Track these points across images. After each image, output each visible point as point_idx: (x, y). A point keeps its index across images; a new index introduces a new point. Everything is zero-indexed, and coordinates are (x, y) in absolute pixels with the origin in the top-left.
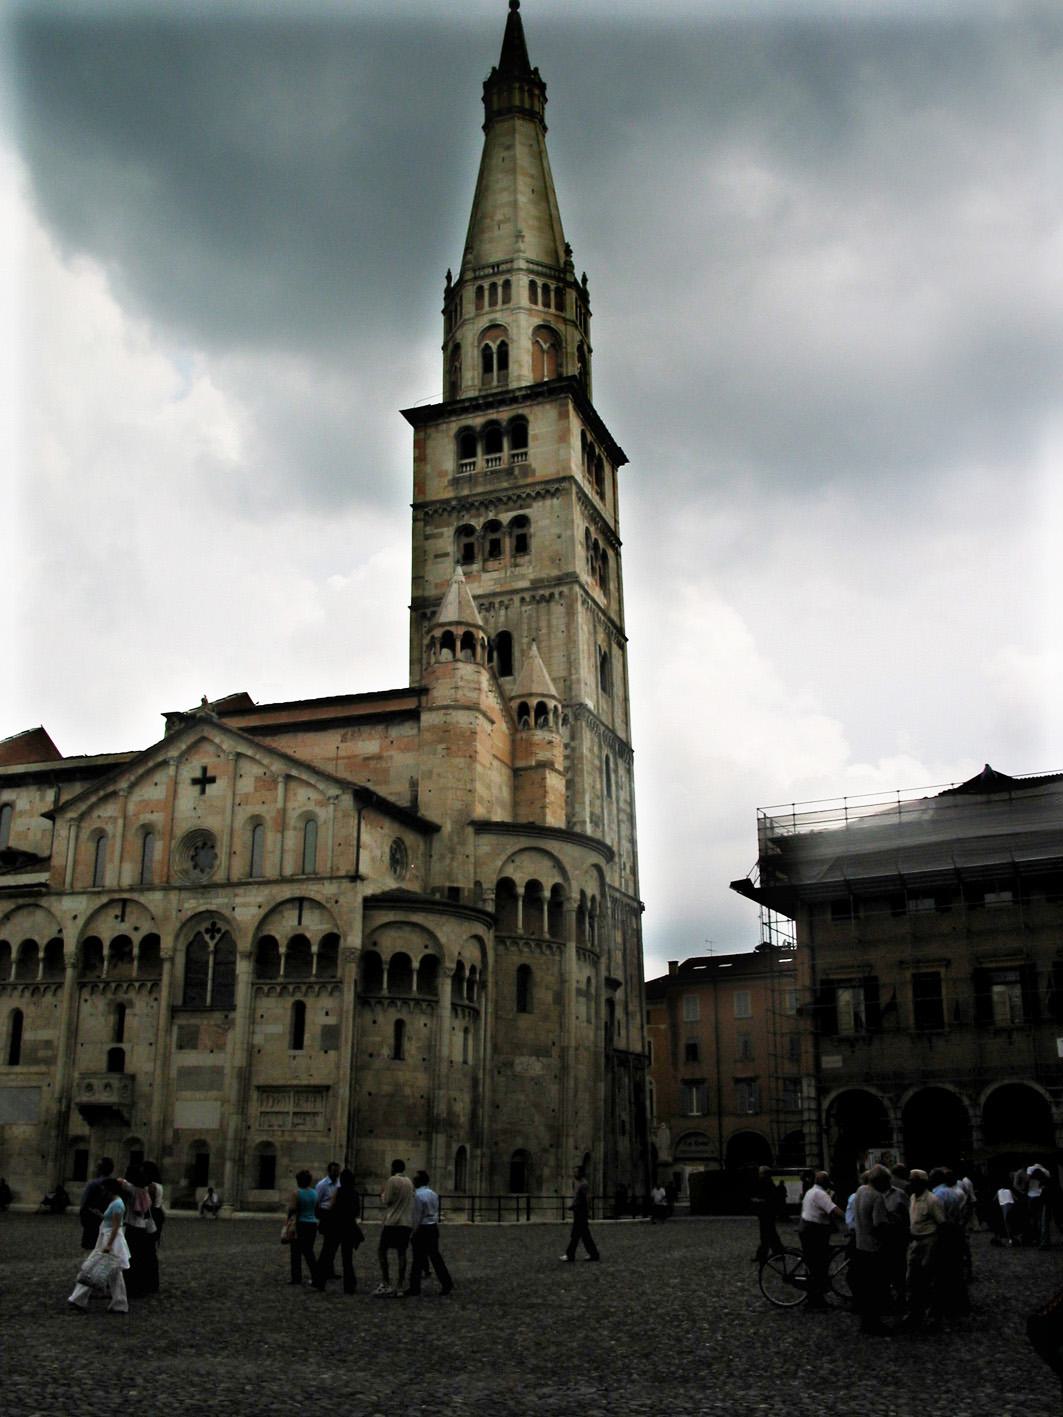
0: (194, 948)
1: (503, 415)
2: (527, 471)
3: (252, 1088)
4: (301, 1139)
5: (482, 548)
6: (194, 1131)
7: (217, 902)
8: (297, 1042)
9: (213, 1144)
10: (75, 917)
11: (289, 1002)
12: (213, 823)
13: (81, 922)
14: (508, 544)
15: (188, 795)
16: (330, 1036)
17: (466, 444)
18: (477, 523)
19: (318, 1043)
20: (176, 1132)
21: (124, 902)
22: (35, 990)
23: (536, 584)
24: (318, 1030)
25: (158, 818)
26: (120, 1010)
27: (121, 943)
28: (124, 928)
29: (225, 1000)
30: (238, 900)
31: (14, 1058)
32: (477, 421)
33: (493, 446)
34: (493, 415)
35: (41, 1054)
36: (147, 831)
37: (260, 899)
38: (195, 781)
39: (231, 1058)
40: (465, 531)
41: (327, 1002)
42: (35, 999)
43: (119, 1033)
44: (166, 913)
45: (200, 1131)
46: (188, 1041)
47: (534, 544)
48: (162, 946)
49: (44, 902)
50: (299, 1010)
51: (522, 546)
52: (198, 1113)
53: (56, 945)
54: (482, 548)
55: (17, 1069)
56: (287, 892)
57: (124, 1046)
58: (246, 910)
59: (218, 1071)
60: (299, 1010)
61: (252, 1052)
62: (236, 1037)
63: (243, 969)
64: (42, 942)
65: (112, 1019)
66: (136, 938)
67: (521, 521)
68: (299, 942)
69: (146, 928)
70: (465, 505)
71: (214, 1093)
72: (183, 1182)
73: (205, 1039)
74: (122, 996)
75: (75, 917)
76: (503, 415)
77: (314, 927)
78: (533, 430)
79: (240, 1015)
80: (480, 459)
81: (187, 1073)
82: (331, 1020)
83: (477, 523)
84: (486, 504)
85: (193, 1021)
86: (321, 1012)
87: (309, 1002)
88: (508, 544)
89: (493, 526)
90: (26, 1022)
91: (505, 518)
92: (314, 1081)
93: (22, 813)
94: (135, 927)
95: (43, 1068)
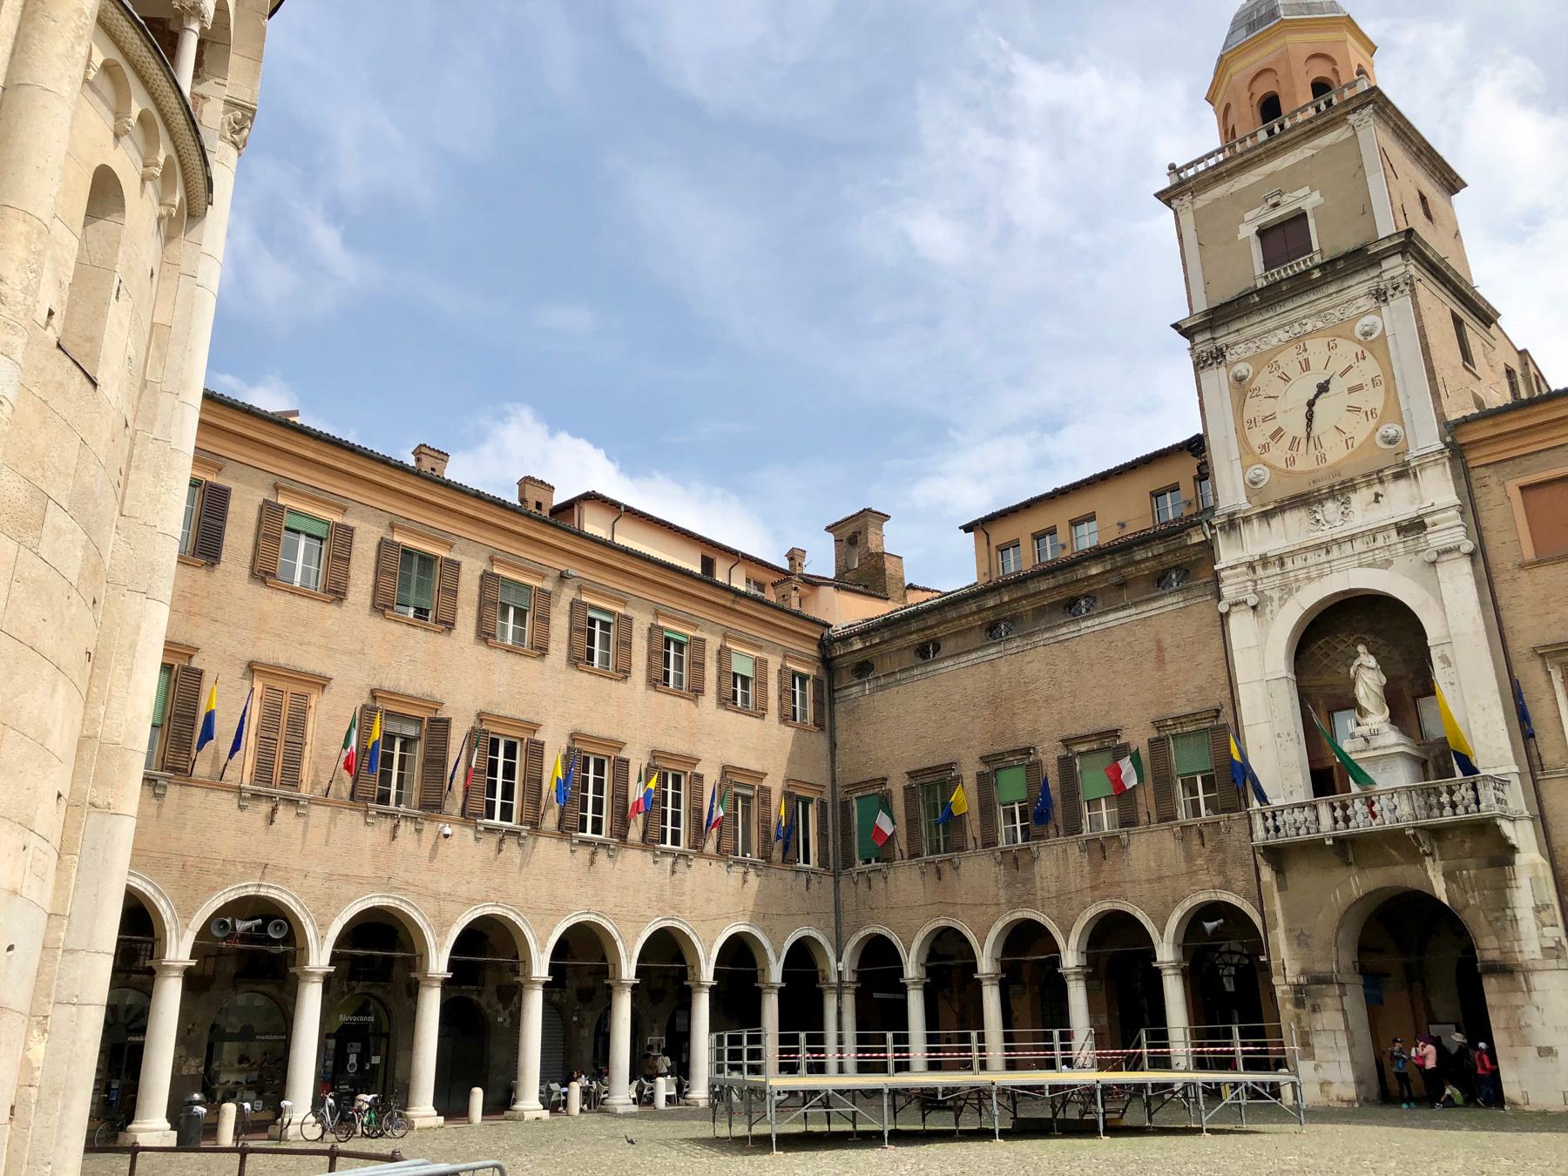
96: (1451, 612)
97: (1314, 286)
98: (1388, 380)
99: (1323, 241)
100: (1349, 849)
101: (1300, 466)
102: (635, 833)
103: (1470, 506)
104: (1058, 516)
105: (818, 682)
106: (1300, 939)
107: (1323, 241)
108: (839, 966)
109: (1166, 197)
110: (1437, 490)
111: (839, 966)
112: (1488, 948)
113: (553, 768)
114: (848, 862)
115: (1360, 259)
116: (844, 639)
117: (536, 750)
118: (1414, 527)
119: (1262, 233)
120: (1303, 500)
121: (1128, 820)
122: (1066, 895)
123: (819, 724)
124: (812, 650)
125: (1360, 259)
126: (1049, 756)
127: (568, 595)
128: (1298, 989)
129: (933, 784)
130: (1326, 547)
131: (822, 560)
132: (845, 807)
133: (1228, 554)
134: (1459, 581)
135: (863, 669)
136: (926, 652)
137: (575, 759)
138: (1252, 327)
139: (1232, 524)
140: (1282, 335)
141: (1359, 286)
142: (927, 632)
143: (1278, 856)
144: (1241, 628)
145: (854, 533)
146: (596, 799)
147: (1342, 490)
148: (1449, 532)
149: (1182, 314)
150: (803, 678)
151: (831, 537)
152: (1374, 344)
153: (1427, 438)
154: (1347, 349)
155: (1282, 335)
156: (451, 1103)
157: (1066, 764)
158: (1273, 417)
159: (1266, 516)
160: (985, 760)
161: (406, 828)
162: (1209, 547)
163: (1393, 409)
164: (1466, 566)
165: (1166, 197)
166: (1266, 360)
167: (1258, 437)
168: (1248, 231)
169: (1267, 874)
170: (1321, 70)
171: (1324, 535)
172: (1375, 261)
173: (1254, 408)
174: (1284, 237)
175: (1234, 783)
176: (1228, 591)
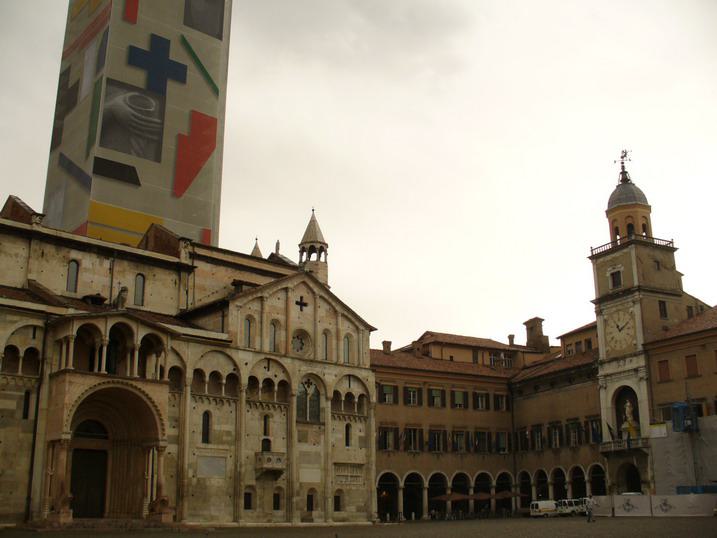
4: (354, 488)
6: (309, 484)
7: (317, 370)
8: (347, 444)
9: (319, 490)
10: (246, 364)
11: (345, 423)
12: (308, 328)
13: (250, 366)
15: (294, 309)
19: (357, 444)
20: (301, 484)
21: (269, 360)
22: (219, 401)
24: (357, 438)
25: (281, 318)
26: (266, 418)
27: (268, 382)
28: (269, 374)
29: (317, 418)
30: (326, 371)
31: (206, 439)
35: (225, 438)
36: (275, 323)
37: (335, 372)
38: (297, 303)
42: (218, 406)
43: (266, 433)
45: (313, 484)
46: (303, 439)
48: (293, 388)
49: (228, 351)
52: (309, 475)
55: (210, 446)
56: (347, 371)
57: (271, 438)
58: (331, 376)
59: (318, 454)
60: (348, 427)
65: (263, 422)
66: (276, 381)
68: (349, 396)
69: (281, 376)
71: (317, 466)
72: (306, 509)
73: (311, 438)
74: (266, 411)
75: (246, 364)
77: (356, 390)
81: (304, 454)
82: (362, 434)
85: (306, 429)
86: (358, 429)
87: (353, 424)
90: (214, 419)
92: (357, 462)
93: (86, 270)
94: (278, 377)
95: (226, 447)
96: (642, 392)
97: (623, 295)
98: (634, 327)
99: (624, 284)
100: (619, 453)
101: (618, 348)
102: (449, 449)
103: (648, 366)
104: (582, 338)
105: (507, 396)
106: (611, 475)
107: (624, 284)
108: (515, 481)
109: (590, 258)
110: (641, 362)
111: (515, 481)
112: (642, 478)
113: (426, 437)
114: (517, 449)
115: (629, 291)
116: (515, 383)
117: (421, 432)
118: (636, 370)
119: (612, 274)
120: (616, 359)
121: (580, 443)
122: (566, 462)
123: (508, 409)
124: (505, 387)
125: (629, 291)
126: (564, 423)
127: (427, 386)
128: (610, 487)
129: (538, 427)
130: (620, 373)
131: (522, 340)
132: (516, 435)
133: (601, 372)
134: (644, 385)
135: (520, 392)
136: (536, 388)
137: (431, 432)
139: (602, 363)
140: (614, 309)
141: (630, 298)
142: (535, 385)
143: (606, 454)
144: (602, 393)
145: (534, 326)
146: (436, 442)
147: (624, 358)
148: (642, 374)
149: (594, 297)
150: (502, 396)
151: (525, 327)
152: (632, 315)
153: (640, 348)
154: (627, 316)
155: (614, 309)
156: (408, 516)
157: (567, 426)
158: (611, 333)
159: (609, 362)
160: (550, 424)
161: (392, 454)
162: (597, 369)
163: (635, 337)
164: (645, 383)
165: (590, 258)
166: (611, 315)
167: (609, 339)
168: (608, 274)
169: (606, 459)
170: (629, 221)
171: (620, 369)
172: (634, 291)
173: (609, 329)
174: (616, 276)
175: (598, 436)
176: (600, 383)
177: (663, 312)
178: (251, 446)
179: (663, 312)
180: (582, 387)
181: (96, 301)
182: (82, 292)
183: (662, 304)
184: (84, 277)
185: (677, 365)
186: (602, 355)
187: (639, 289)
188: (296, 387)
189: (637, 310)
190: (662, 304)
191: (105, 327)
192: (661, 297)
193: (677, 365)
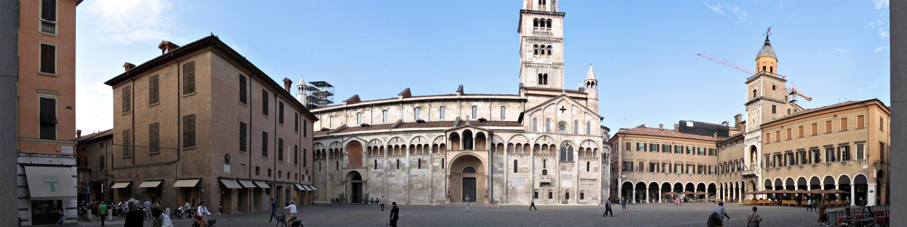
0: (563, 150)
1: (546, 18)
2: (551, 34)
3: (580, 180)
5: (539, 52)
14: (546, 52)
16: (596, 169)
17: (536, 23)
18: (540, 45)
23: (554, 64)
32: (539, 17)
33: (542, 25)
34: (543, 17)
39: (574, 173)
40: (536, 46)
41: (595, 162)
44: (557, 140)
47: (553, 53)
50: (588, 163)
51: (549, 53)
53: (527, 145)
54: (539, 52)
58: (577, 142)
61: (579, 171)
62: (575, 168)
63: (576, 154)
64: (523, 144)
67: (549, 47)
69: (552, 143)
70: (536, 39)
76: (546, 18)
78: (553, 24)
79: (576, 164)
80: (539, 27)
83: (540, 45)
84: (542, 40)
88: (546, 52)
89: (543, 46)
91: (546, 45)
115: (758, 100)
138: (751, 106)
141: (758, 103)
148: (760, 139)
177: (774, 111)
178: (539, 171)
179: (774, 111)
180: (738, 146)
181: (482, 121)
182: (479, 117)
183: (774, 107)
184: (478, 112)
185: (773, 136)
186: (747, 131)
187: (762, 98)
188: (558, 147)
189: (760, 109)
190: (774, 107)
191: (460, 132)
192: (775, 103)
193: (773, 136)
